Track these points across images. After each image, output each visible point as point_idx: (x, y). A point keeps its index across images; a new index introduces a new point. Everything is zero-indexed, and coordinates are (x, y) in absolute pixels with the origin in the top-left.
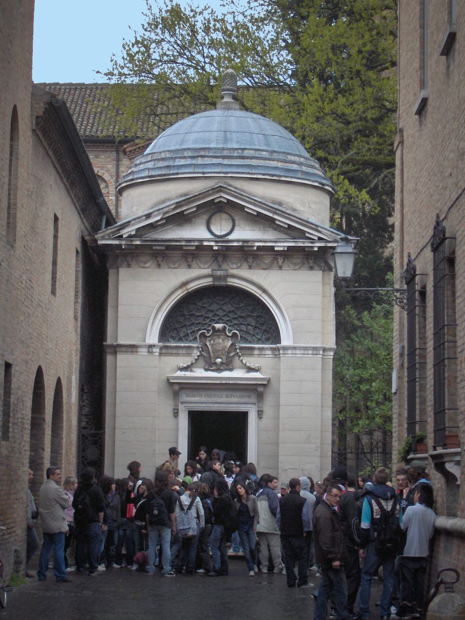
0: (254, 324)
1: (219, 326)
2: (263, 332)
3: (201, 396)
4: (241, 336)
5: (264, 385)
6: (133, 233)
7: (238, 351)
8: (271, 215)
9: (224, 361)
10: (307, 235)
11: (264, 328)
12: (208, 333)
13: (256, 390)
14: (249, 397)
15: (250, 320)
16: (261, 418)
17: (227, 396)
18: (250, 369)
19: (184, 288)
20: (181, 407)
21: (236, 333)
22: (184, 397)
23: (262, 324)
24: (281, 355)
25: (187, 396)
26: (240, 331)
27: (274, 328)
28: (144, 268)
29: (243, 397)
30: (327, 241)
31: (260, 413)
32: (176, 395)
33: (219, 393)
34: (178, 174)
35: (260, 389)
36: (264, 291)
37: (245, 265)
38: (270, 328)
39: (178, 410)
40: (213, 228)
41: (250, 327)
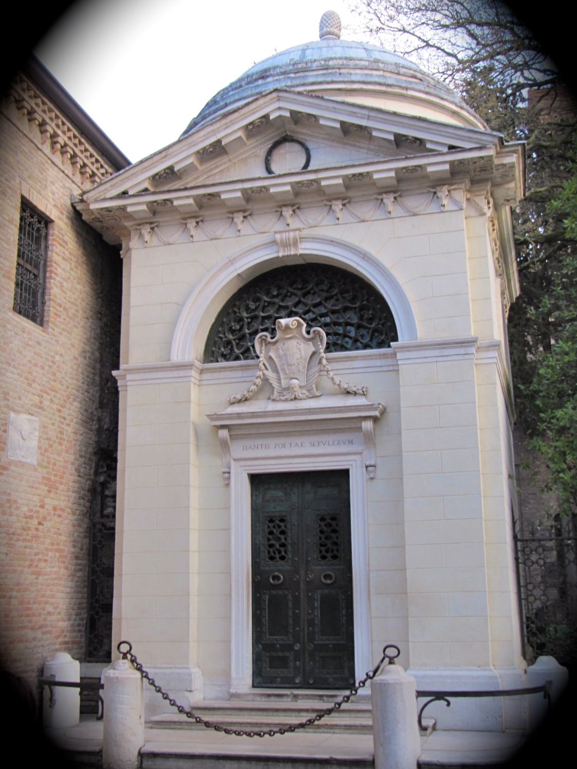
0: (355, 320)
1: (283, 321)
2: (373, 335)
4: (328, 334)
5: (375, 419)
6: (146, 185)
7: (324, 362)
8: (364, 123)
9: (302, 384)
10: (429, 146)
11: (373, 325)
12: (272, 338)
14: (351, 442)
15: (349, 314)
16: (372, 479)
18: (348, 393)
19: (232, 268)
21: (319, 333)
22: (238, 449)
23: (370, 320)
25: (245, 448)
26: (320, 327)
27: (389, 324)
28: (169, 244)
30: (464, 150)
31: (370, 469)
32: (224, 445)
33: (299, 440)
34: (226, 105)
35: (368, 425)
36: (365, 256)
37: (329, 220)
39: (229, 473)
40: (275, 168)
41: (348, 328)
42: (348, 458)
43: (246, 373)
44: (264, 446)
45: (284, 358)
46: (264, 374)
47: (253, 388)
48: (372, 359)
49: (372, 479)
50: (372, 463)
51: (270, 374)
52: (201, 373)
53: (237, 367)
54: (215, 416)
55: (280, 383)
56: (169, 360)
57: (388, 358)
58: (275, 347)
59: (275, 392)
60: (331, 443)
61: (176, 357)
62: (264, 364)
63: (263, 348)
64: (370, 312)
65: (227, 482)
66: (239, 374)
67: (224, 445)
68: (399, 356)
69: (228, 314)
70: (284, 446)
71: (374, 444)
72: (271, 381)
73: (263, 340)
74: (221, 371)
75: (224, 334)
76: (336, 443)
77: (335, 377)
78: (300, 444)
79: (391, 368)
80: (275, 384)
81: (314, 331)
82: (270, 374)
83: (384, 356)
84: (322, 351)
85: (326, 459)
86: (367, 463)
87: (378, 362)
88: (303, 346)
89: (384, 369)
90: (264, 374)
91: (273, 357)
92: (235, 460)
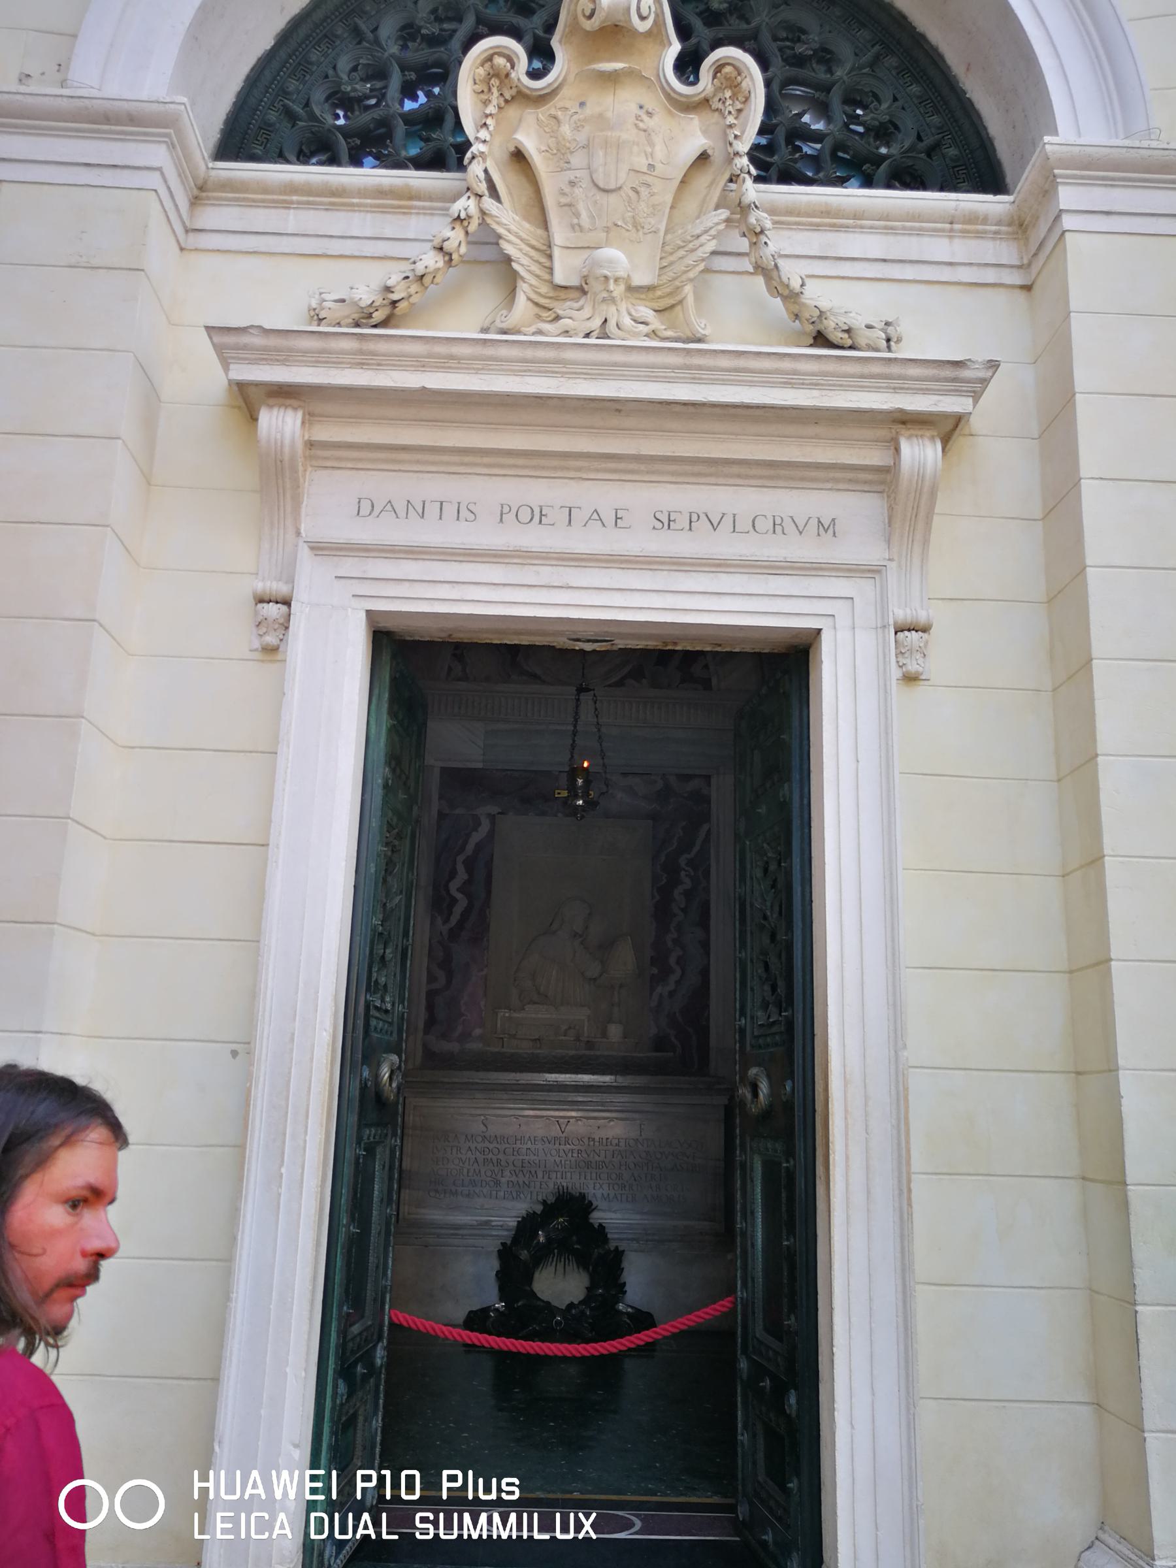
3: (465, 512)
5: (949, 430)
12: (534, 75)
13: (882, 479)
14: (827, 528)
16: (910, 679)
17: (666, 522)
18: (821, 339)
20: (313, 584)
21: (731, 81)
23: (884, 132)
24: (1068, 222)
25: (365, 508)
27: (952, 152)
29: (776, 526)
32: (277, 481)
35: (919, 454)
38: (930, 152)
39: (287, 603)
42: (817, 586)
43: (391, 225)
44: (450, 510)
45: (577, 160)
46: (483, 213)
47: (431, 261)
48: (920, 232)
49: (910, 679)
50: (922, 617)
51: (507, 217)
52: (195, 201)
53: (363, 192)
54: (257, 340)
55: (551, 270)
56: (63, 84)
57: (980, 235)
58: (543, 112)
59: (521, 299)
60: (744, 524)
61: (98, 77)
62: (486, 171)
63: (491, 109)
64: (884, 106)
65: (271, 639)
66: (361, 223)
67: (277, 481)
68: (1067, 196)
69: (330, 38)
70: (540, 516)
71: (926, 542)
72: (509, 250)
73: (496, 76)
74: (287, 205)
75: (307, 105)
76: (764, 525)
77: (781, 263)
78: (609, 518)
79: (990, 276)
80: (524, 263)
81: (719, 68)
82: (507, 217)
83: (971, 225)
84: (744, 147)
85: (725, 582)
86: (901, 614)
87: (939, 248)
88: (661, 122)
89: (965, 275)
90: (483, 213)
91: (530, 143)
92: (319, 548)
